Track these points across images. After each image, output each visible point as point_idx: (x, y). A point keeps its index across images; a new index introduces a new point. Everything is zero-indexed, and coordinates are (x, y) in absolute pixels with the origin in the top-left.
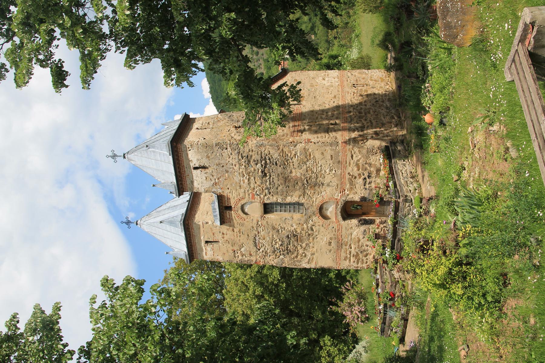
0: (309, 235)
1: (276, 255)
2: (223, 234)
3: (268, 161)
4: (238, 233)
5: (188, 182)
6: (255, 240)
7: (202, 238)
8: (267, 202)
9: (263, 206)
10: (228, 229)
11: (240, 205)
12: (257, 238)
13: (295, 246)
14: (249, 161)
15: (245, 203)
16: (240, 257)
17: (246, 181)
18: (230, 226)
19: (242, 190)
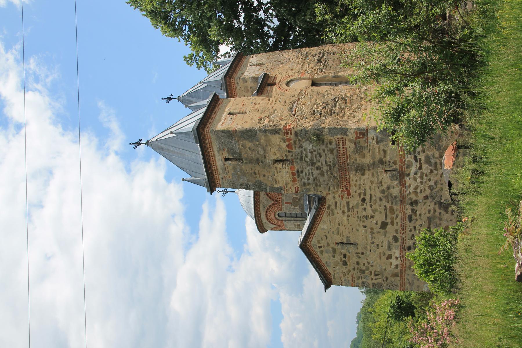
0: (361, 98)
1: (314, 117)
2: (255, 104)
3: (326, 54)
4: (274, 102)
5: (240, 73)
6: (293, 106)
7: (227, 110)
8: (316, 77)
9: (311, 82)
10: (262, 100)
11: (286, 81)
12: (295, 105)
13: (341, 108)
14: (307, 56)
15: (292, 81)
16: (266, 123)
17: (299, 66)
18: (267, 97)
19: (294, 71)
